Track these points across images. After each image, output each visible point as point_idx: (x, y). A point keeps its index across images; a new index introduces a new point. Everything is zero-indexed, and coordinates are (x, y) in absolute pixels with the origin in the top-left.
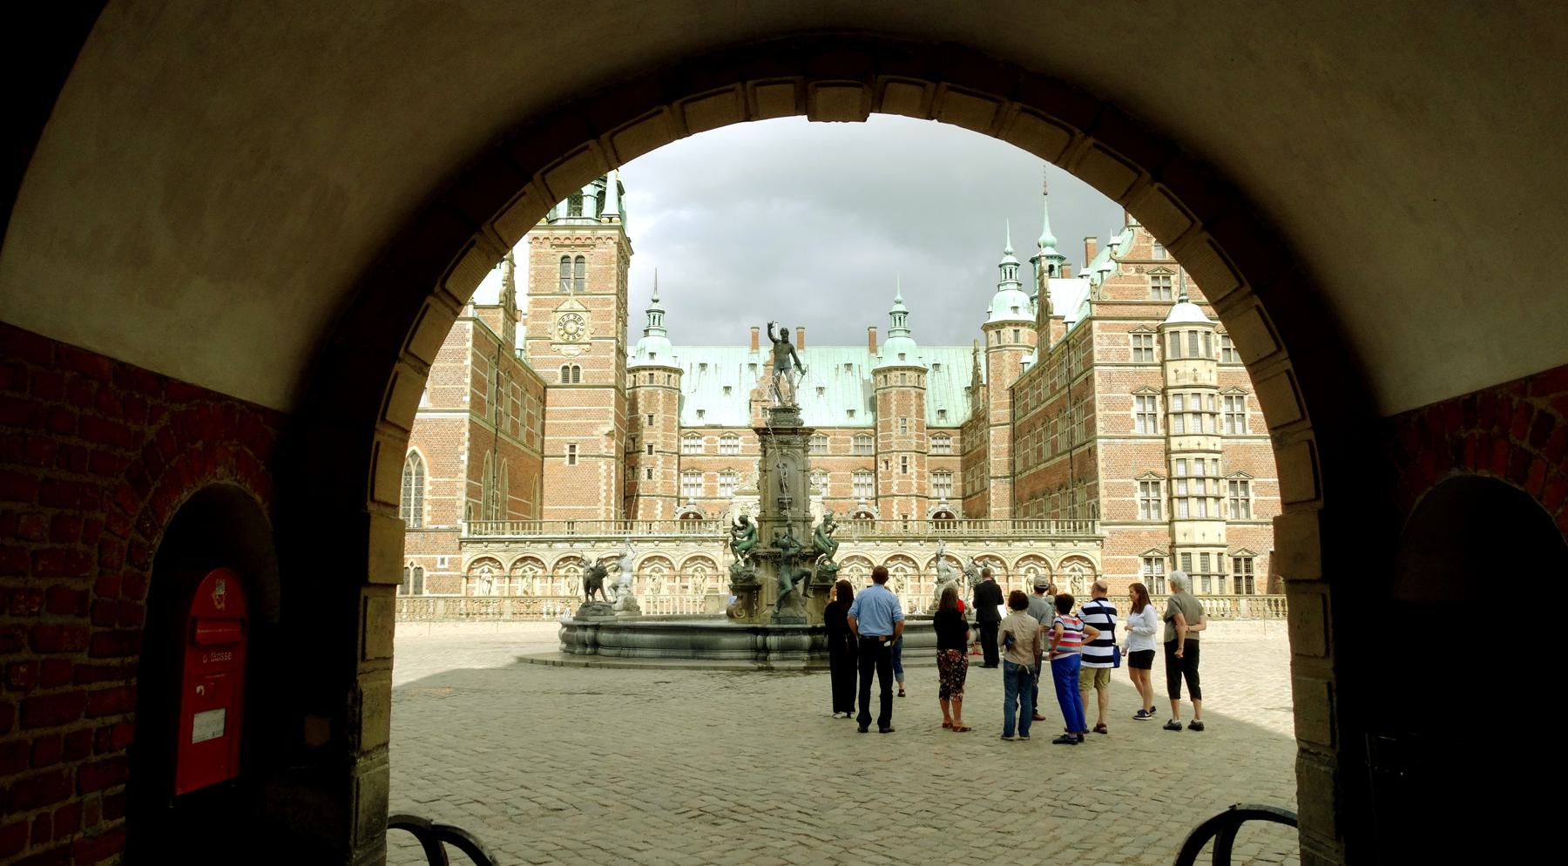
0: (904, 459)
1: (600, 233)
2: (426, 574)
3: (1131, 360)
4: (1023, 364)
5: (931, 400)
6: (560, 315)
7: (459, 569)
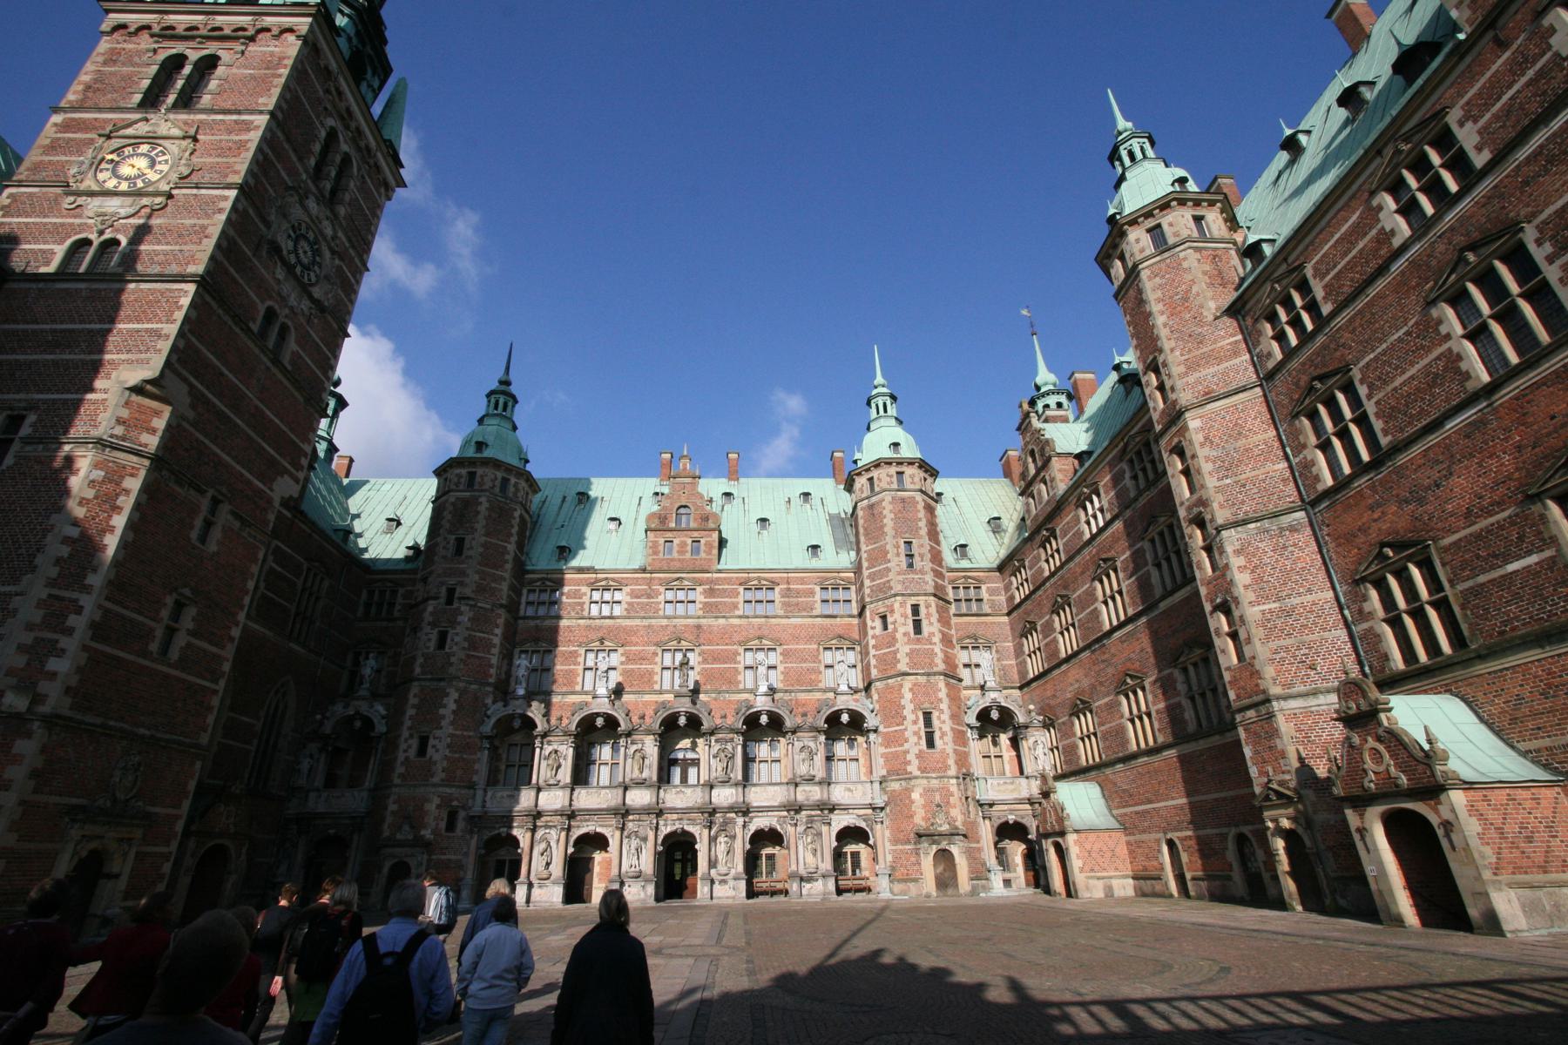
0: (915, 609)
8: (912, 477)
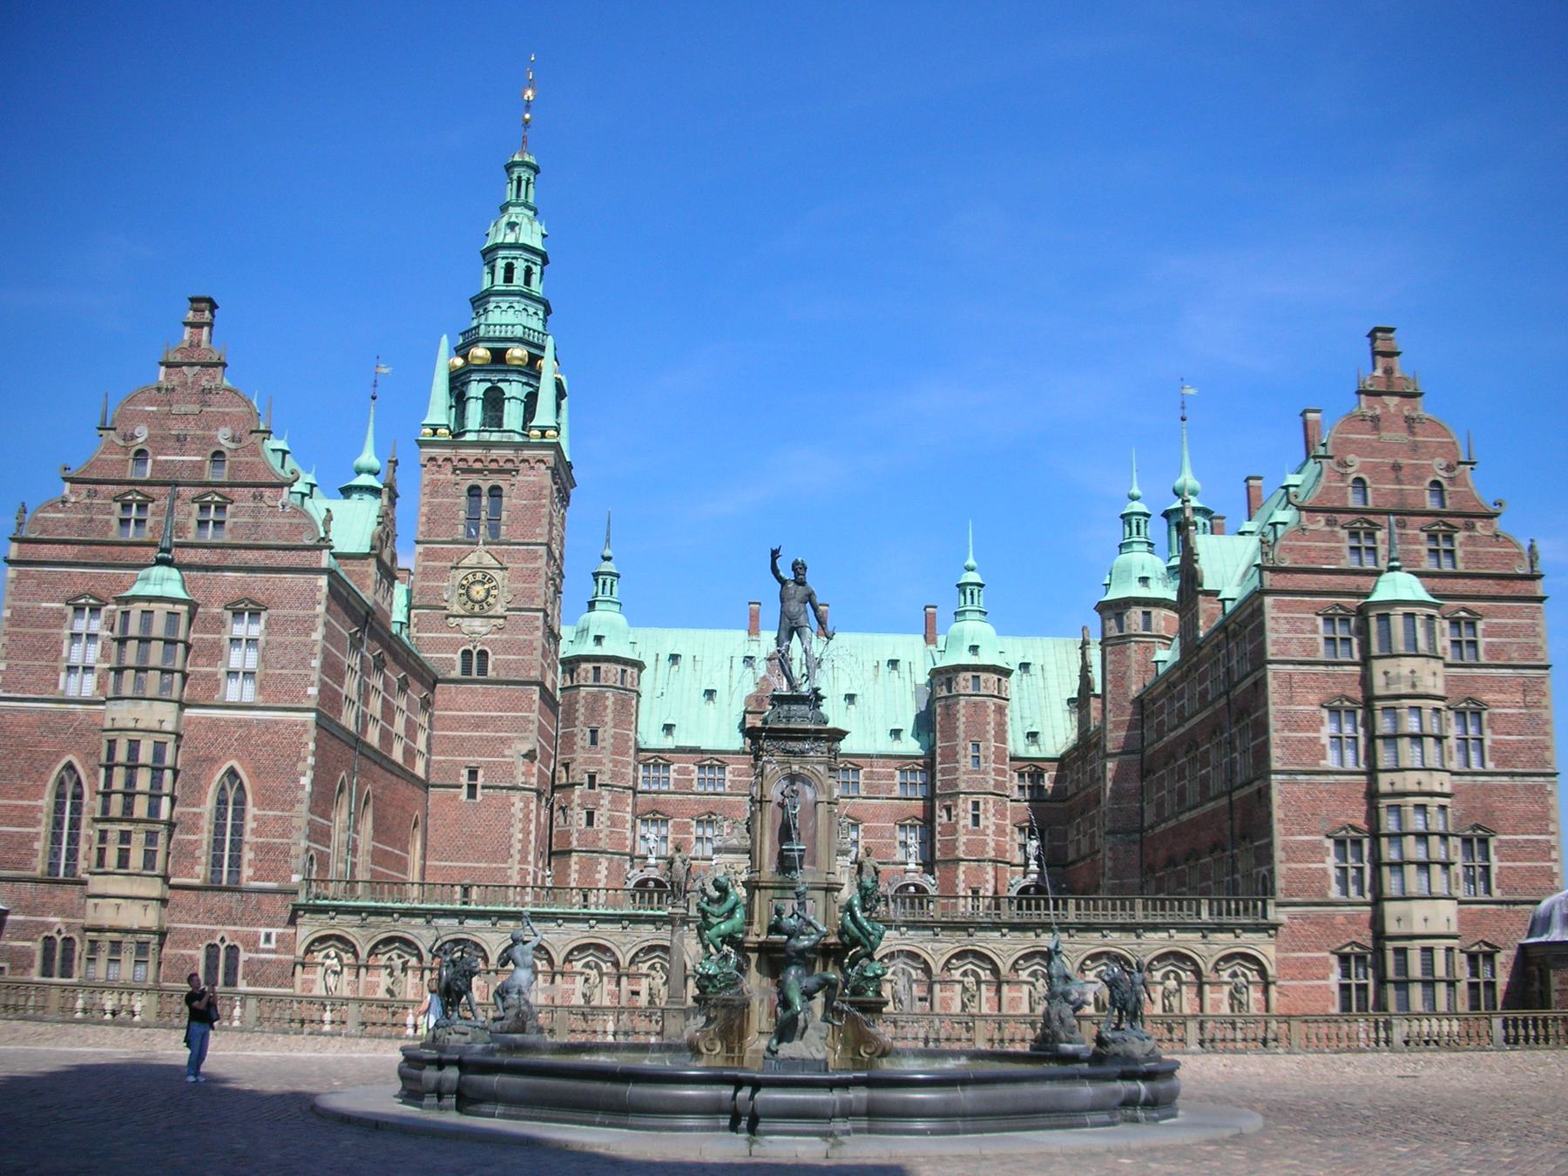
0: (976, 805)
1: (527, 453)
2: (243, 956)
3: (1321, 655)
4: (1157, 662)
5: (1017, 716)
6: (463, 573)
7: (292, 951)
8: (986, 681)
